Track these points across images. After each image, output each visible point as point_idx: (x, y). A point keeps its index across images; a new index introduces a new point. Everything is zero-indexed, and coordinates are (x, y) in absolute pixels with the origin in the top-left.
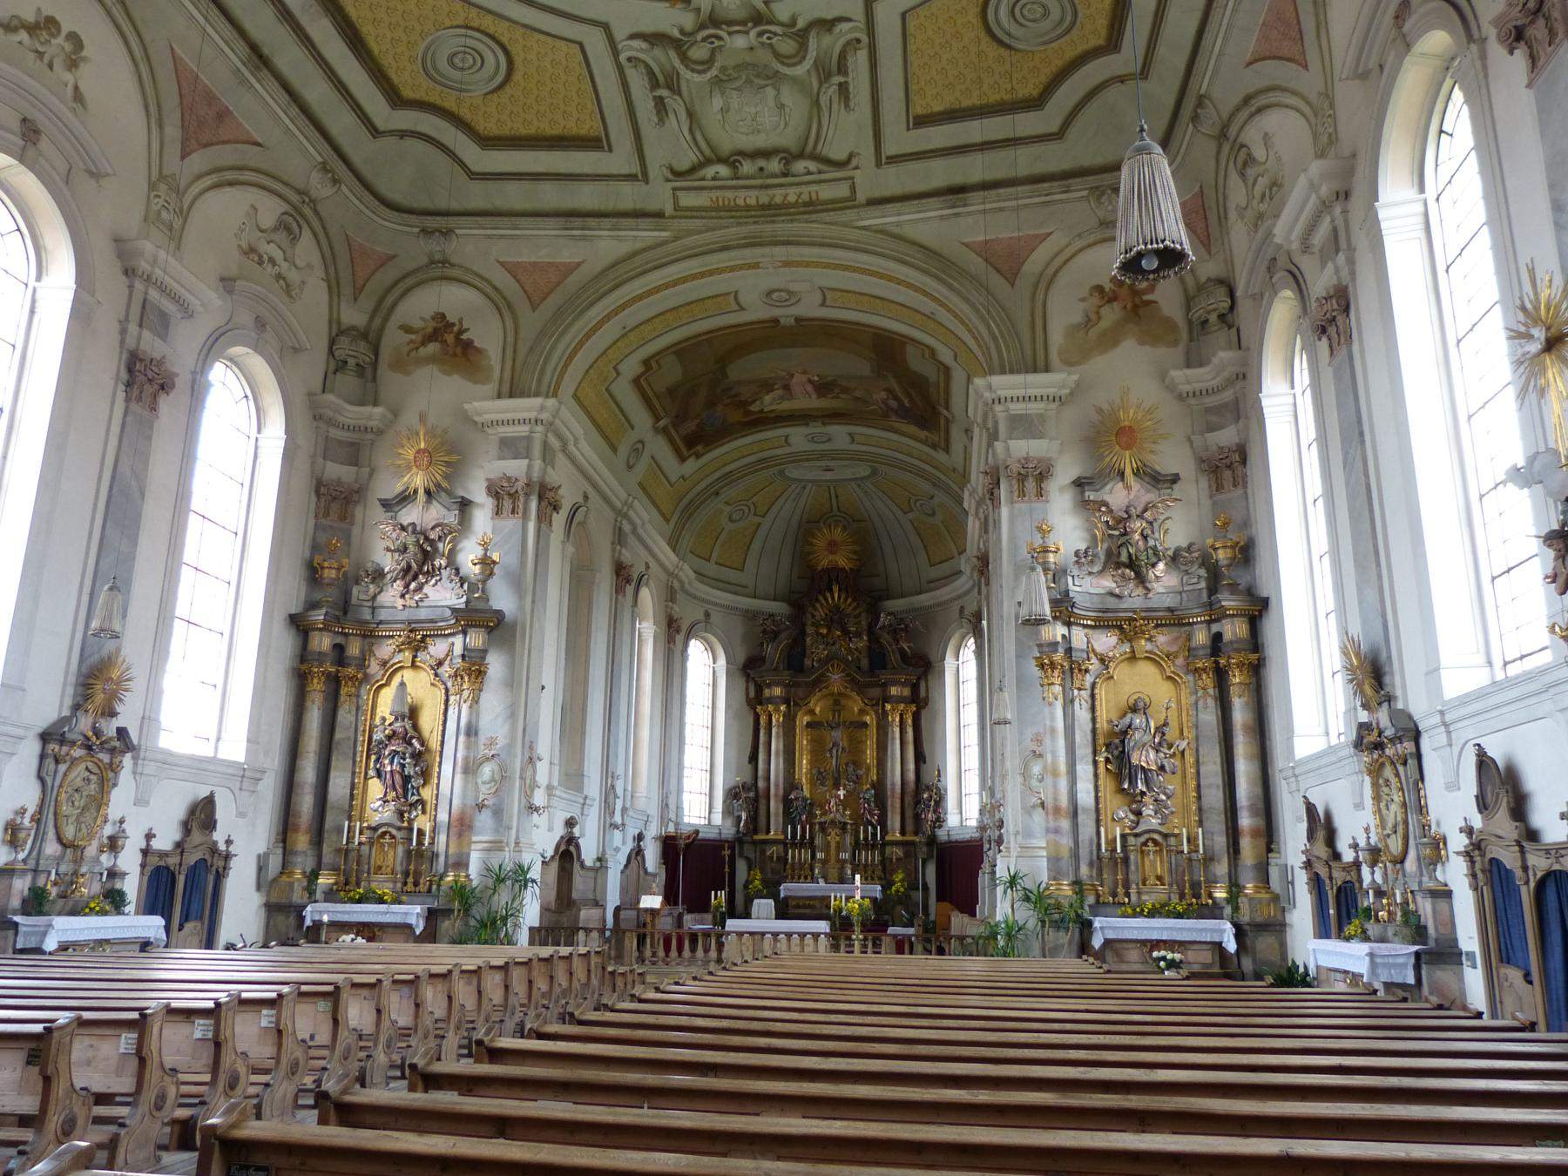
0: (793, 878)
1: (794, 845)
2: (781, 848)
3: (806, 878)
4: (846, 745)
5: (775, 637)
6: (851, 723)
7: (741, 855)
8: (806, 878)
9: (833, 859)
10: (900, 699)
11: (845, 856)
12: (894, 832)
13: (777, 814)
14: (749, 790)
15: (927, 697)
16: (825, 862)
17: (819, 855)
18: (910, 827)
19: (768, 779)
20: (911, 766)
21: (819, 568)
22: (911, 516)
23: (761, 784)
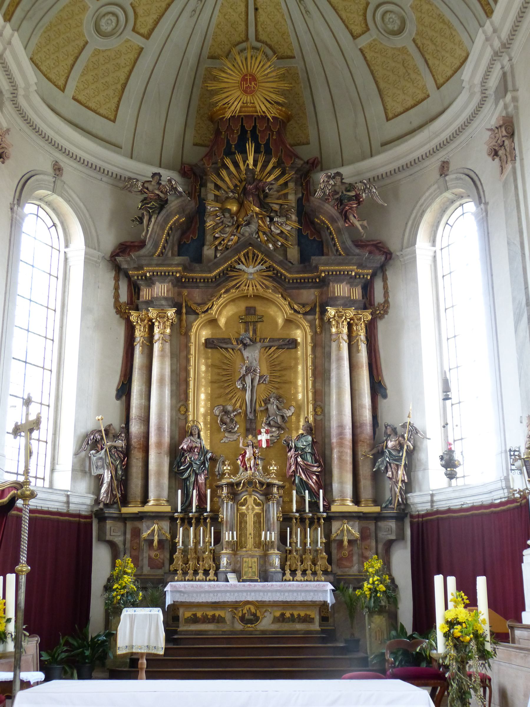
0: (185, 573)
1: (186, 521)
2: (166, 525)
3: (206, 573)
4: (265, 371)
5: (162, 207)
6: (272, 340)
7: (101, 539)
8: (206, 573)
10: (348, 303)
11: (272, 536)
12: (343, 500)
13: (159, 473)
14: (116, 437)
15: (387, 302)
17: (227, 536)
18: (366, 492)
19: (146, 420)
21: (228, 115)
22: (364, 41)
23: (135, 428)
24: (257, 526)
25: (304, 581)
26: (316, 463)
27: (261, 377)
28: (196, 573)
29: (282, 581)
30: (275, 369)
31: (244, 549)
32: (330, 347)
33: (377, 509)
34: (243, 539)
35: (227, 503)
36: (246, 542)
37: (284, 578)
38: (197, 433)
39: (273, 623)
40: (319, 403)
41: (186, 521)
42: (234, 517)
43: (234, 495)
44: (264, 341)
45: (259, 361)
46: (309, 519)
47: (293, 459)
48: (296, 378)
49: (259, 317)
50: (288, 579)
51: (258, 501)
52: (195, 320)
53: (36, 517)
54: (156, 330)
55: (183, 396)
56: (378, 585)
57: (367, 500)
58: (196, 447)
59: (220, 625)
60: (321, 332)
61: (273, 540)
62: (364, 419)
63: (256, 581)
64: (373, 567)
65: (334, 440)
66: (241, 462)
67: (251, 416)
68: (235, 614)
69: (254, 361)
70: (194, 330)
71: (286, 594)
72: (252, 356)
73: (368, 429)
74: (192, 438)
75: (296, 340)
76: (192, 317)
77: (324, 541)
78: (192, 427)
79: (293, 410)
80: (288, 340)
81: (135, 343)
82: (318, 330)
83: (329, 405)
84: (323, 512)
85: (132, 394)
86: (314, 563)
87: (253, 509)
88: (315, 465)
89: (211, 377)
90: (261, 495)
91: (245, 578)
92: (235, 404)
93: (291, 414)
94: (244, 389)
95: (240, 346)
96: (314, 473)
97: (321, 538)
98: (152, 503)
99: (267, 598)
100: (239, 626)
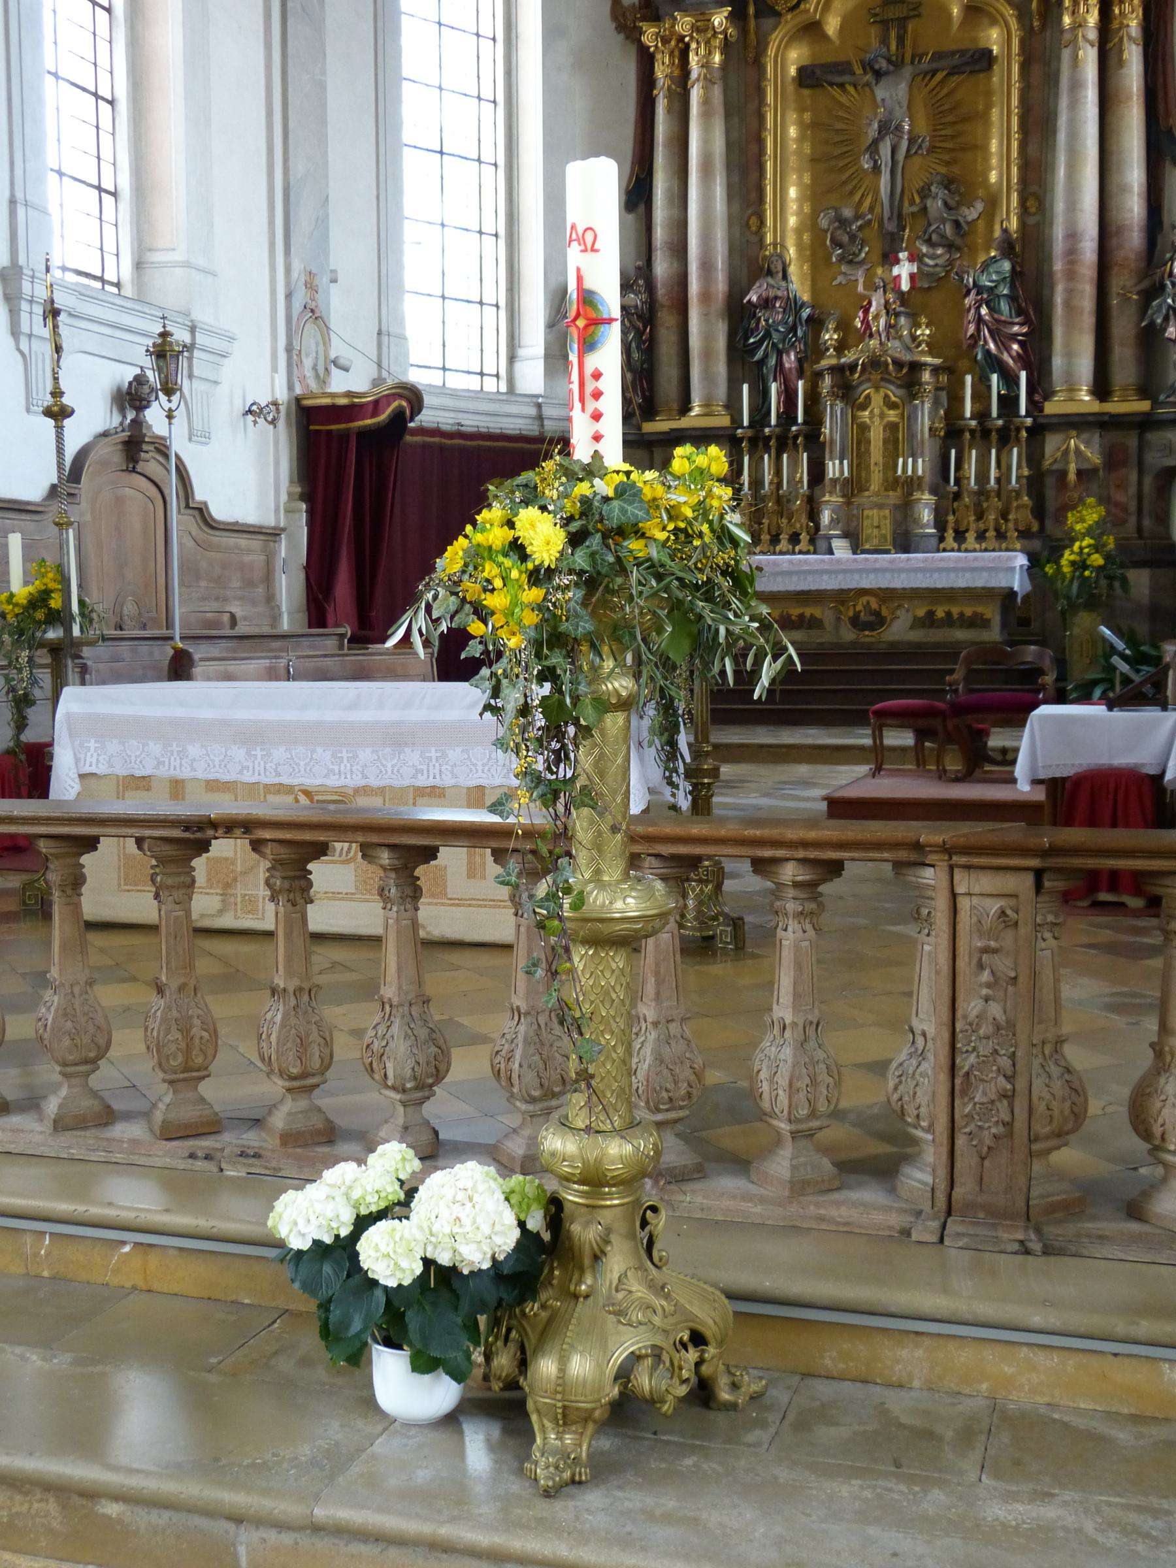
1: (758, 442)
3: (794, 539)
4: (923, 130)
6: (938, 56)
8: (794, 539)
9: (876, 480)
11: (919, 466)
12: (1072, 389)
13: (707, 354)
16: (853, 487)
17: (834, 469)
18: (1125, 370)
19: (680, 250)
20: (1134, 175)
23: (662, 268)
24: (891, 447)
25: (981, 551)
26: (1018, 315)
27: (911, 141)
28: (775, 540)
29: (938, 551)
30: (944, 120)
31: (867, 493)
32: (1059, 59)
33: (1145, 406)
34: (863, 475)
35: (831, 406)
36: (868, 480)
37: (942, 546)
38: (780, 268)
39: (912, 627)
40: (1033, 188)
41: (761, 444)
42: (847, 432)
43: (846, 391)
44: (920, 62)
45: (909, 107)
46: (999, 430)
47: (973, 311)
48: (987, 138)
49: (911, 7)
50: (949, 548)
51: (893, 399)
52: (775, 29)
53: (479, 446)
54: (693, 59)
55: (753, 196)
56: (1089, 555)
57: (1125, 389)
58: (776, 298)
59: (813, 632)
60: (1043, 27)
61: (920, 473)
62: (1128, 215)
63: (887, 552)
64: (1083, 520)
65: (1058, 266)
66: (862, 323)
67: (891, 227)
68: (841, 612)
69: (897, 108)
70: (771, 51)
71: (936, 575)
72: (891, 96)
73: (1134, 239)
74: (770, 280)
75: (991, 51)
76: (768, 22)
77: (1026, 472)
78: (771, 256)
79: (980, 206)
80: (971, 53)
81: (655, 92)
82: (1036, 24)
83: (1052, 191)
84: (1026, 416)
85: (654, 198)
86: (1004, 515)
87: (882, 416)
88: (1017, 320)
89: (812, 149)
90: (899, 387)
91: (867, 547)
92: (860, 202)
93: (975, 216)
94: (876, 169)
95: (869, 77)
96: (1013, 337)
97: (1019, 467)
98: (696, 411)
99: (899, 582)
100: (848, 634)
